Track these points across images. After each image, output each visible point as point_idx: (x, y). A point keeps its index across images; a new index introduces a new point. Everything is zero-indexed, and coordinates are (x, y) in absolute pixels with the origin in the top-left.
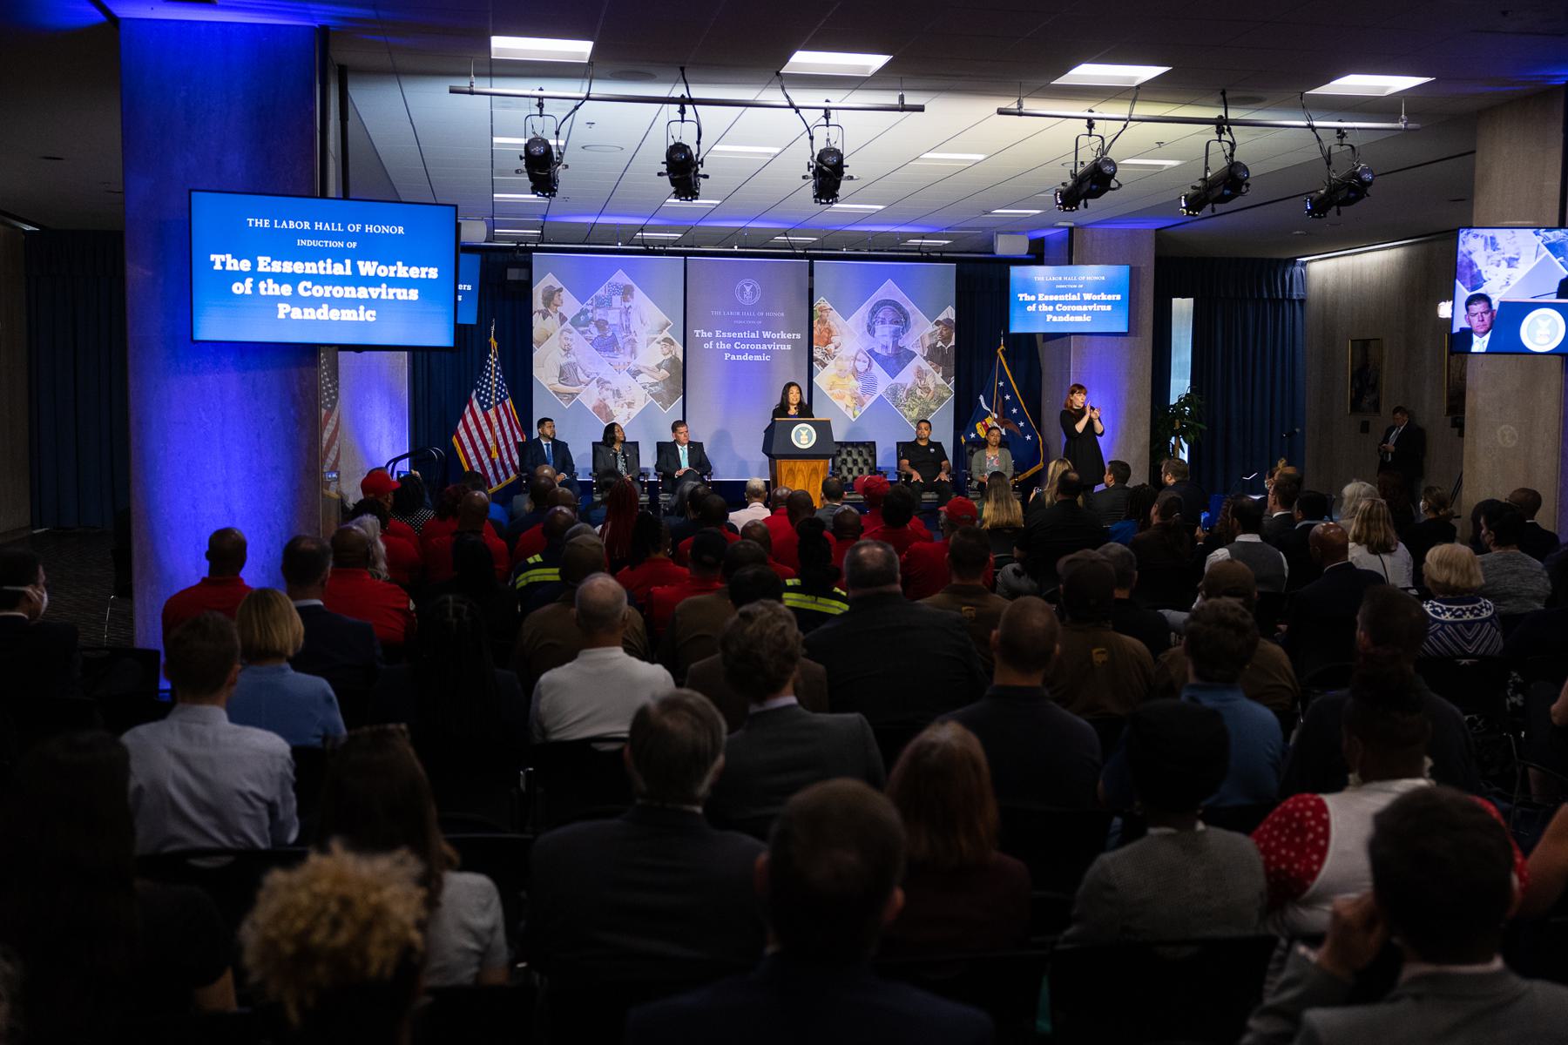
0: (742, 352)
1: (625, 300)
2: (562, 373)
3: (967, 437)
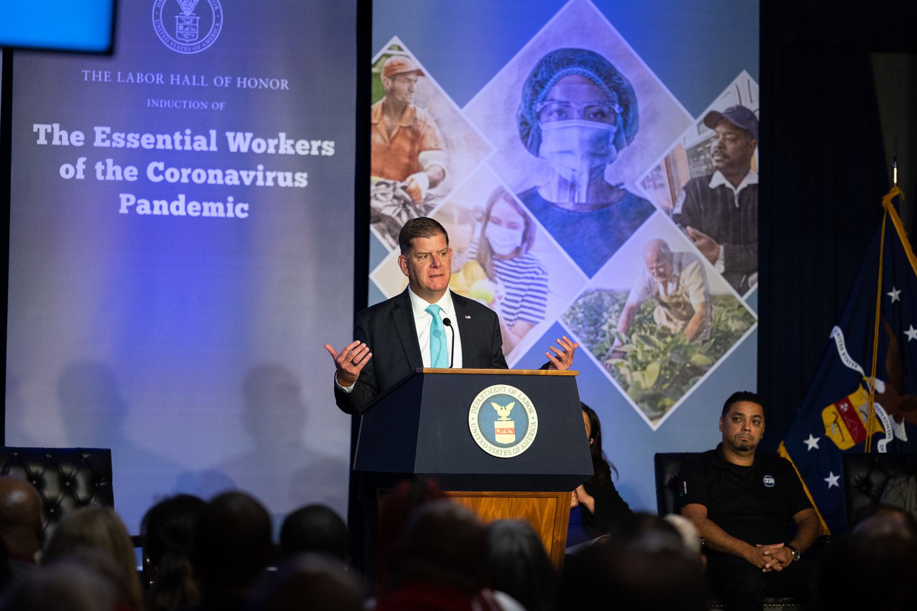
0: (168, 192)
3: (797, 448)
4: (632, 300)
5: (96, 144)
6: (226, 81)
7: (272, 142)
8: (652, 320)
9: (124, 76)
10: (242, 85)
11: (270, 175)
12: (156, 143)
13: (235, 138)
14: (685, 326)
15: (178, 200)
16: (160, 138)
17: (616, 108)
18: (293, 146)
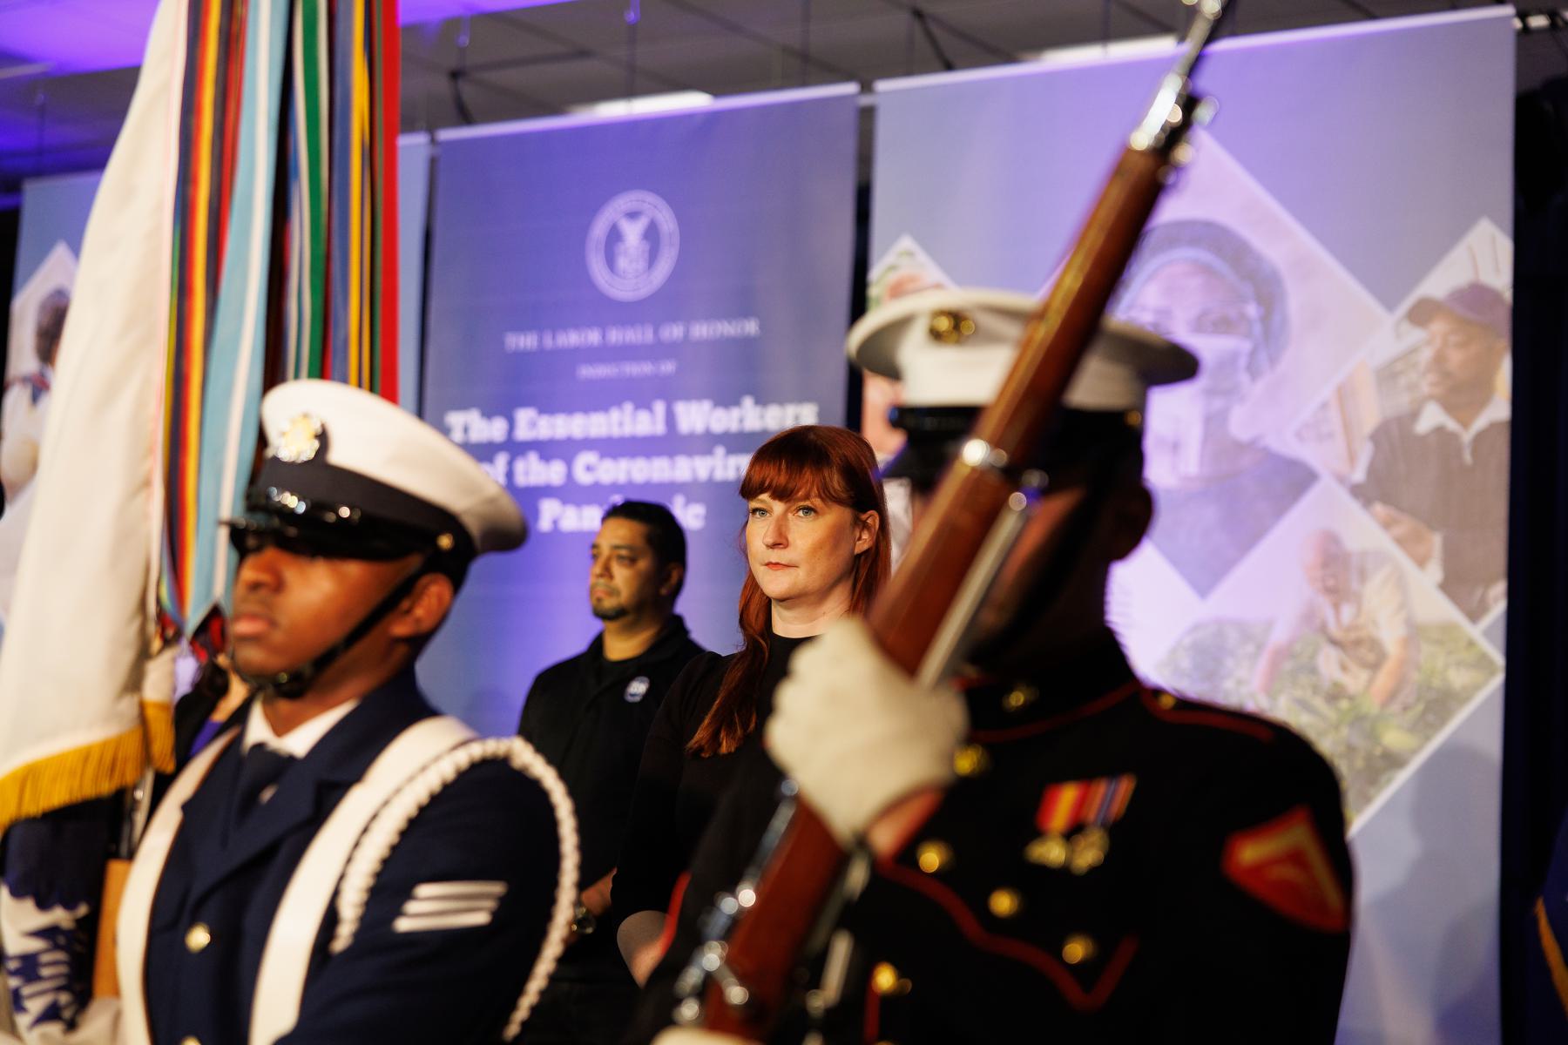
4: (1279, 635)
7: (735, 413)
8: (1313, 670)
14: (1371, 681)
17: (1252, 310)
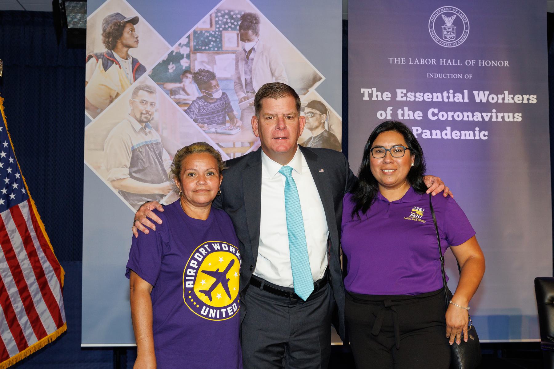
0: (441, 125)
1: (244, 38)
2: (135, 160)
5: (397, 99)
6: (473, 62)
7: (501, 97)
9: (413, 61)
10: (482, 64)
11: (500, 115)
12: (432, 98)
13: (478, 94)
15: (446, 130)
16: (435, 95)
18: (513, 98)
